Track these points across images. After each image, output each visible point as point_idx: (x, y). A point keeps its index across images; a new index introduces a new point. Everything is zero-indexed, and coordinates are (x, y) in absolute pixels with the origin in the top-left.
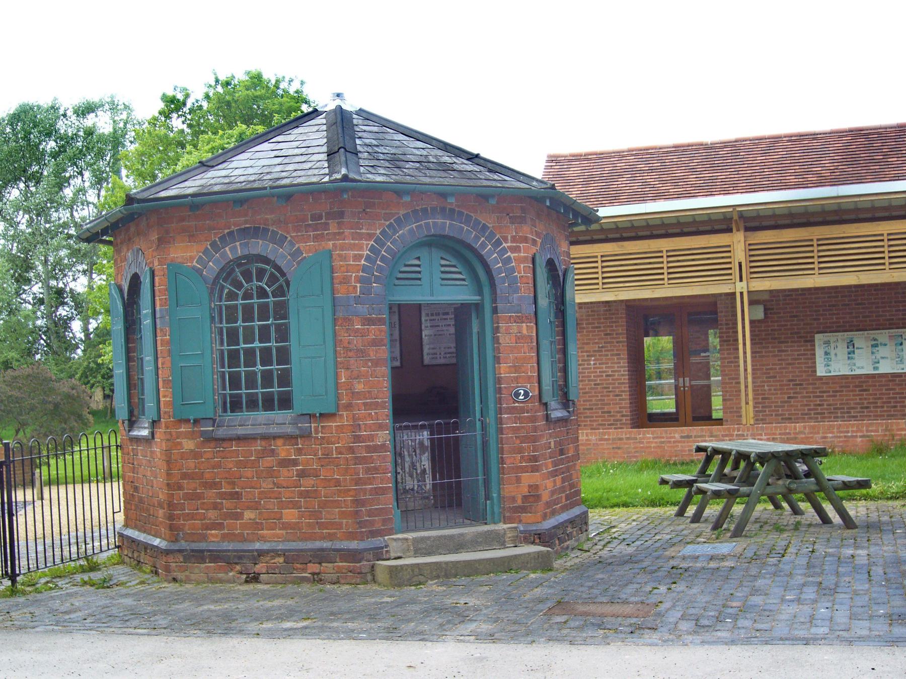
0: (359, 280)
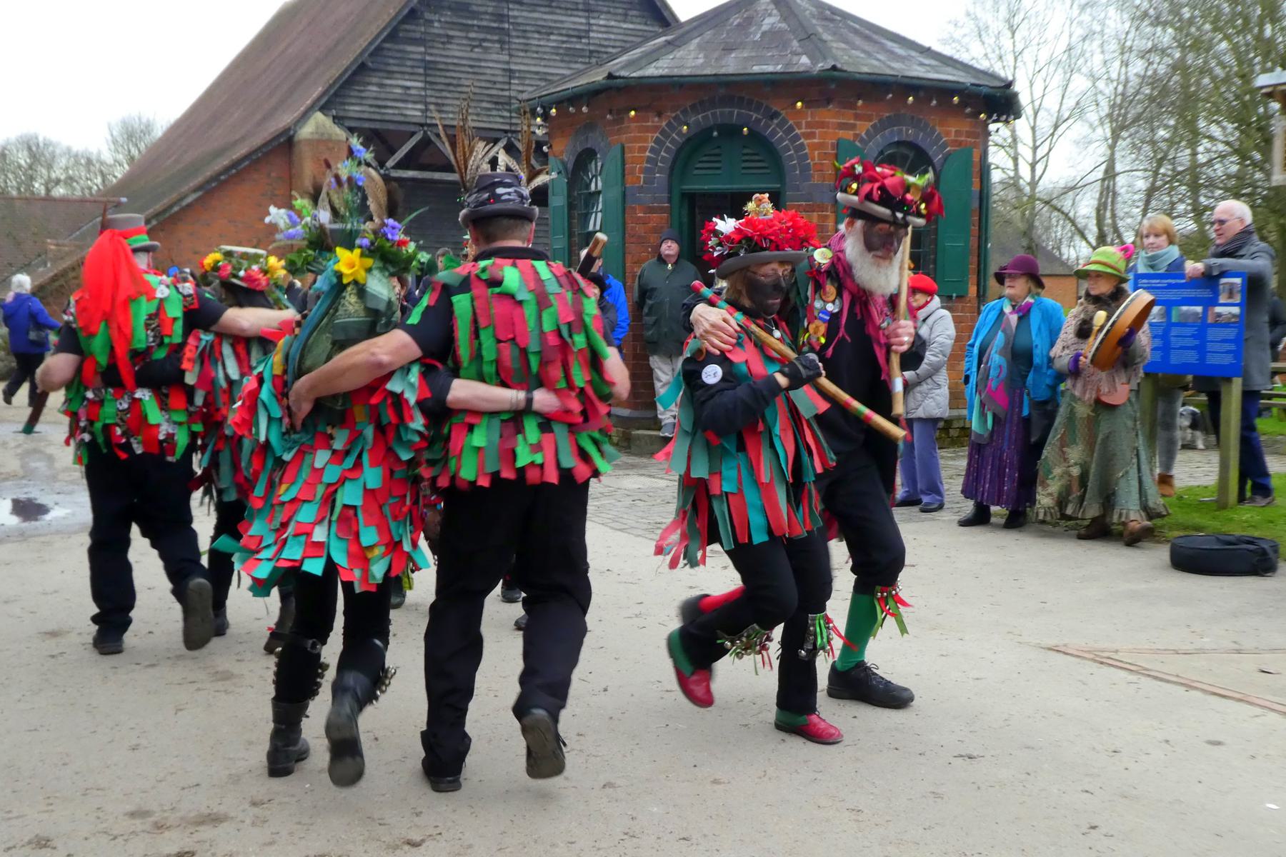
0: (643, 170)
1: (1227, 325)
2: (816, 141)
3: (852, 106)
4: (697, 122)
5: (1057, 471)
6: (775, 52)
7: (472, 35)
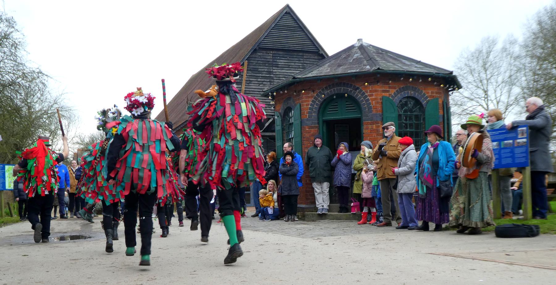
0: (308, 113)
1: (522, 146)
2: (374, 97)
3: (388, 84)
4: (328, 93)
5: (455, 206)
6: (357, 65)
7: (259, 80)
